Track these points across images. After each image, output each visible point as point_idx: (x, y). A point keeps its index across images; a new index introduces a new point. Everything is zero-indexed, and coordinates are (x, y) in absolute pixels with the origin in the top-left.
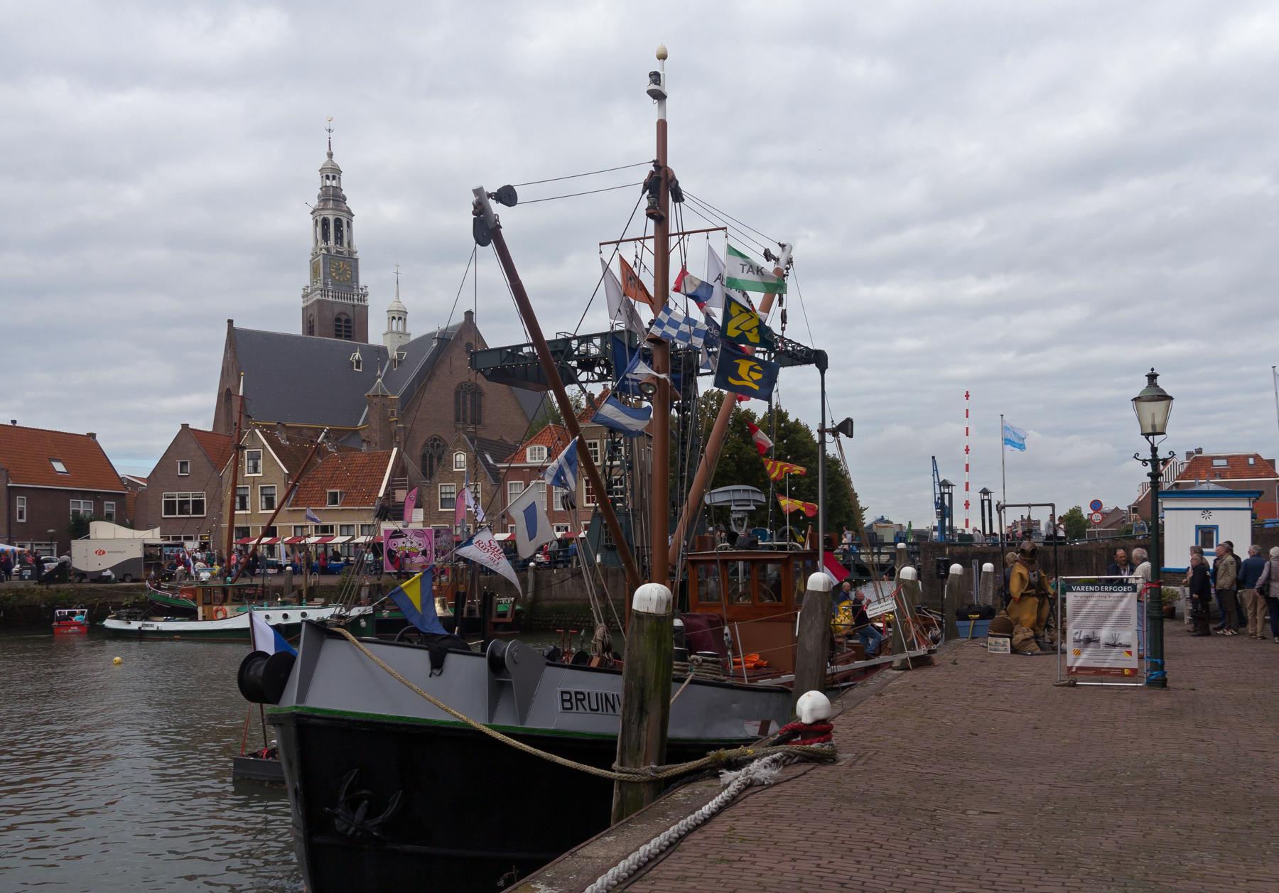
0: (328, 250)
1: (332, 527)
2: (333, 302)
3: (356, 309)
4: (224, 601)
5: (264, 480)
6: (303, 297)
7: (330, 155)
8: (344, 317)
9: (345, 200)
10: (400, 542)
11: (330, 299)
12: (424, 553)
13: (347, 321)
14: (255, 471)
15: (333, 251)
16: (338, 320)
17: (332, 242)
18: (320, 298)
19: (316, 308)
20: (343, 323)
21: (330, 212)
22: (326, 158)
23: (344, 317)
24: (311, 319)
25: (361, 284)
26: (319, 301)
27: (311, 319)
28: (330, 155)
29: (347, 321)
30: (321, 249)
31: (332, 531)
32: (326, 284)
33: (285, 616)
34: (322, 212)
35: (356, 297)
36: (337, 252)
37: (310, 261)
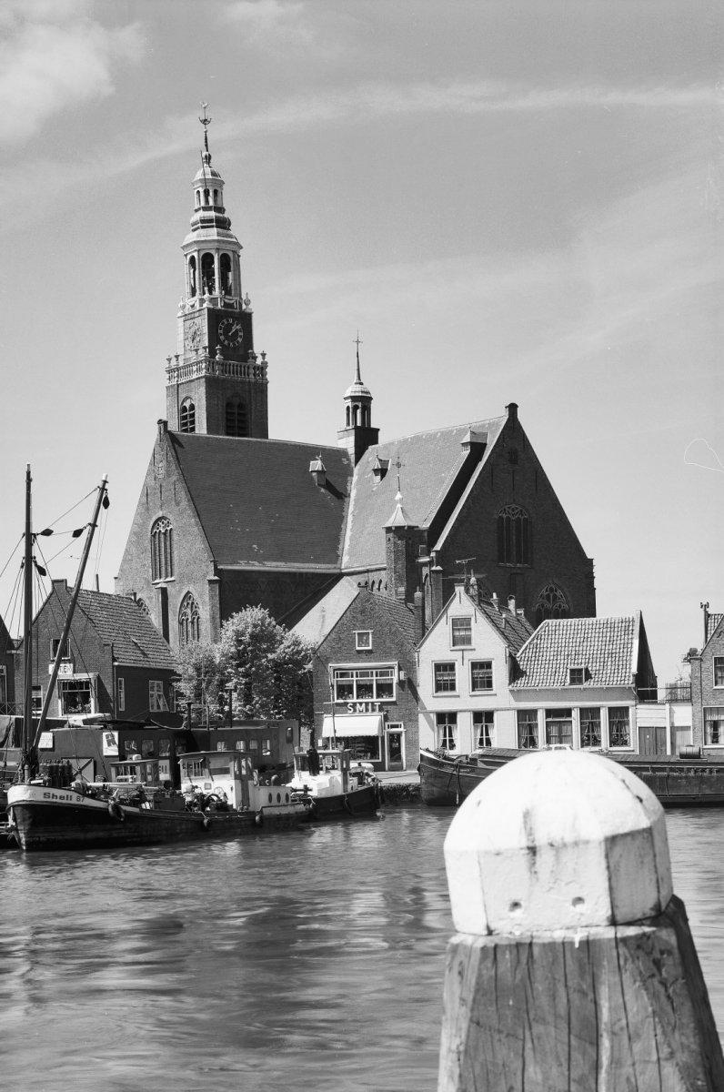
0: (213, 300)
6: (170, 371)
8: (236, 401)
9: (230, 224)
13: (241, 406)
16: (229, 405)
17: (217, 293)
20: (236, 410)
23: (236, 401)
24: (187, 404)
25: (257, 349)
27: (187, 404)
29: (241, 406)
31: (570, 715)
35: (252, 371)
36: (226, 305)
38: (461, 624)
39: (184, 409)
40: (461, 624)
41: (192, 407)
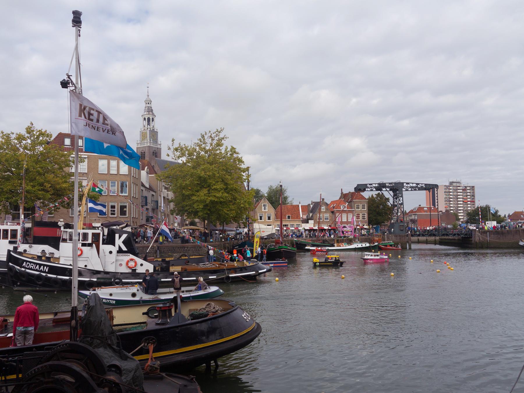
1: (288, 225)
2: (153, 147)
3: (158, 149)
4: (343, 242)
5: (268, 212)
7: (148, 96)
8: (155, 152)
10: (345, 229)
11: (152, 146)
12: (351, 231)
13: (156, 153)
14: (265, 210)
15: (152, 129)
16: (153, 153)
18: (149, 145)
19: (147, 148)
21: (151, 116)
22: (147, 97)
23: (155, 152)
24: (143, 152)
26: (149, 146)
27: (143, 152)
28: (148, 96)
30: (148, 128)
32: (150, 140)
33: (362, 245)
34: (148, 115)
36: (153, 130)
37: (140, 132)
38: (264, 206)
39: (142, 153)
40: (264, 206)
41: (144, 152)
